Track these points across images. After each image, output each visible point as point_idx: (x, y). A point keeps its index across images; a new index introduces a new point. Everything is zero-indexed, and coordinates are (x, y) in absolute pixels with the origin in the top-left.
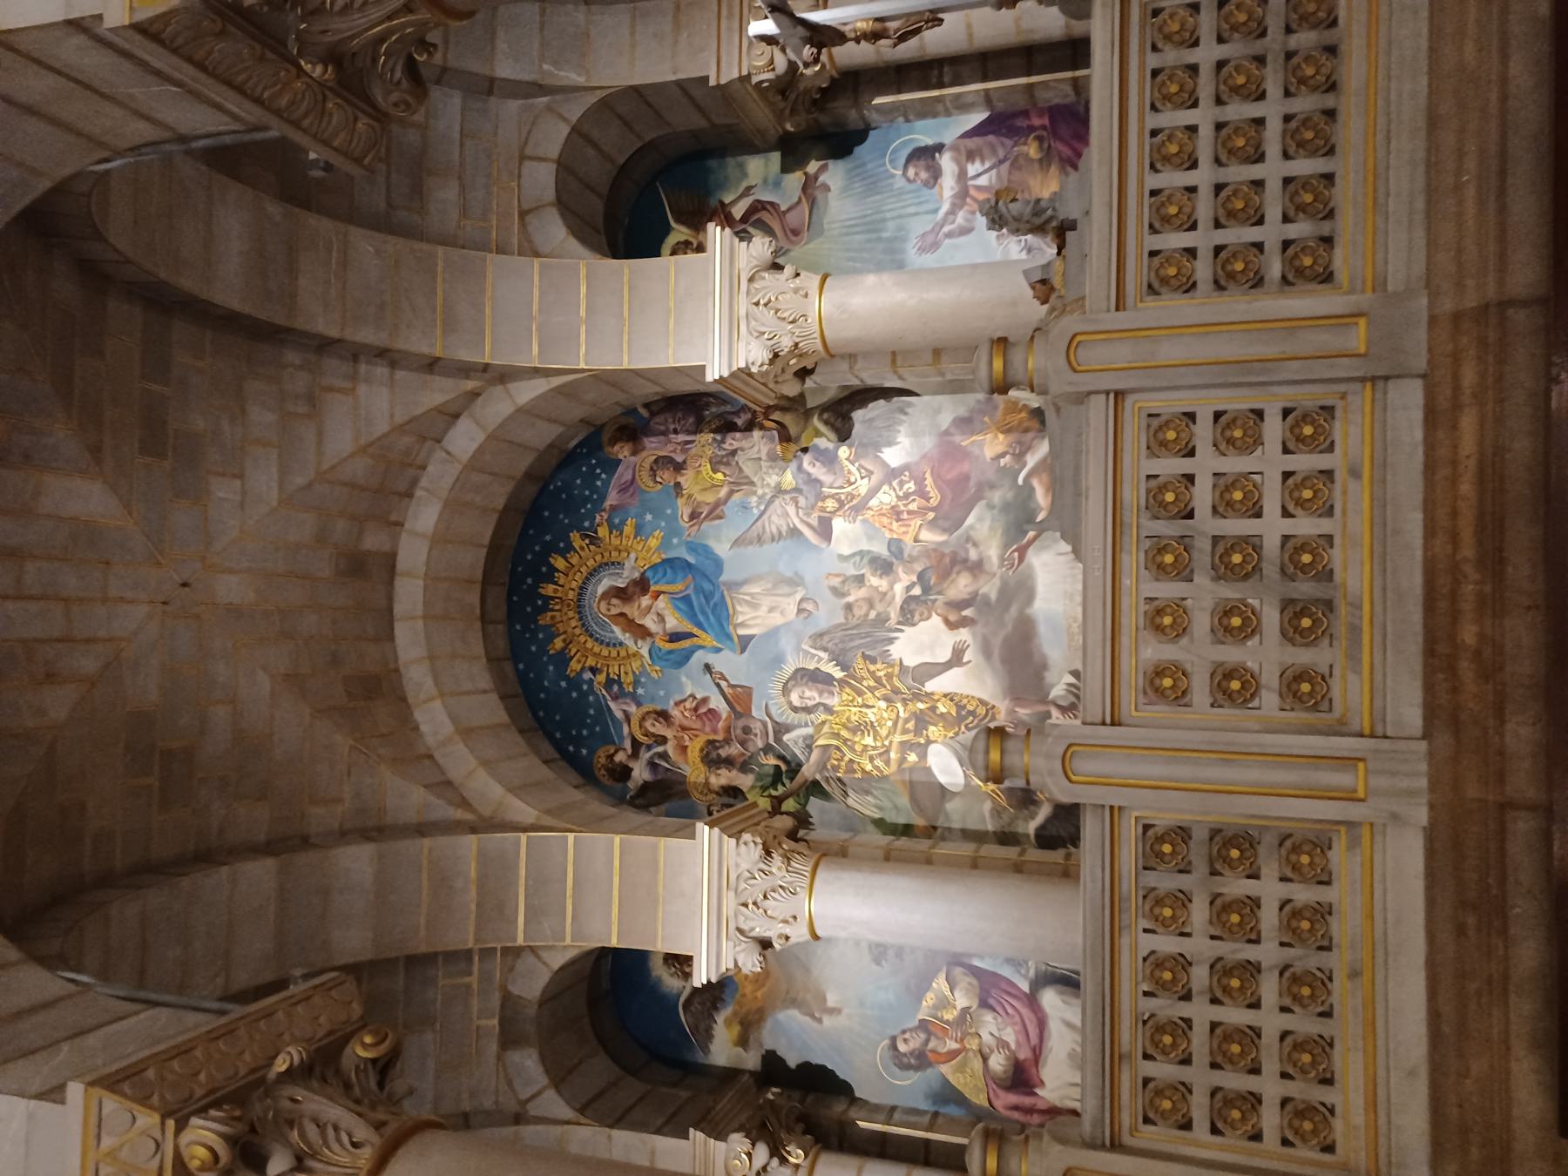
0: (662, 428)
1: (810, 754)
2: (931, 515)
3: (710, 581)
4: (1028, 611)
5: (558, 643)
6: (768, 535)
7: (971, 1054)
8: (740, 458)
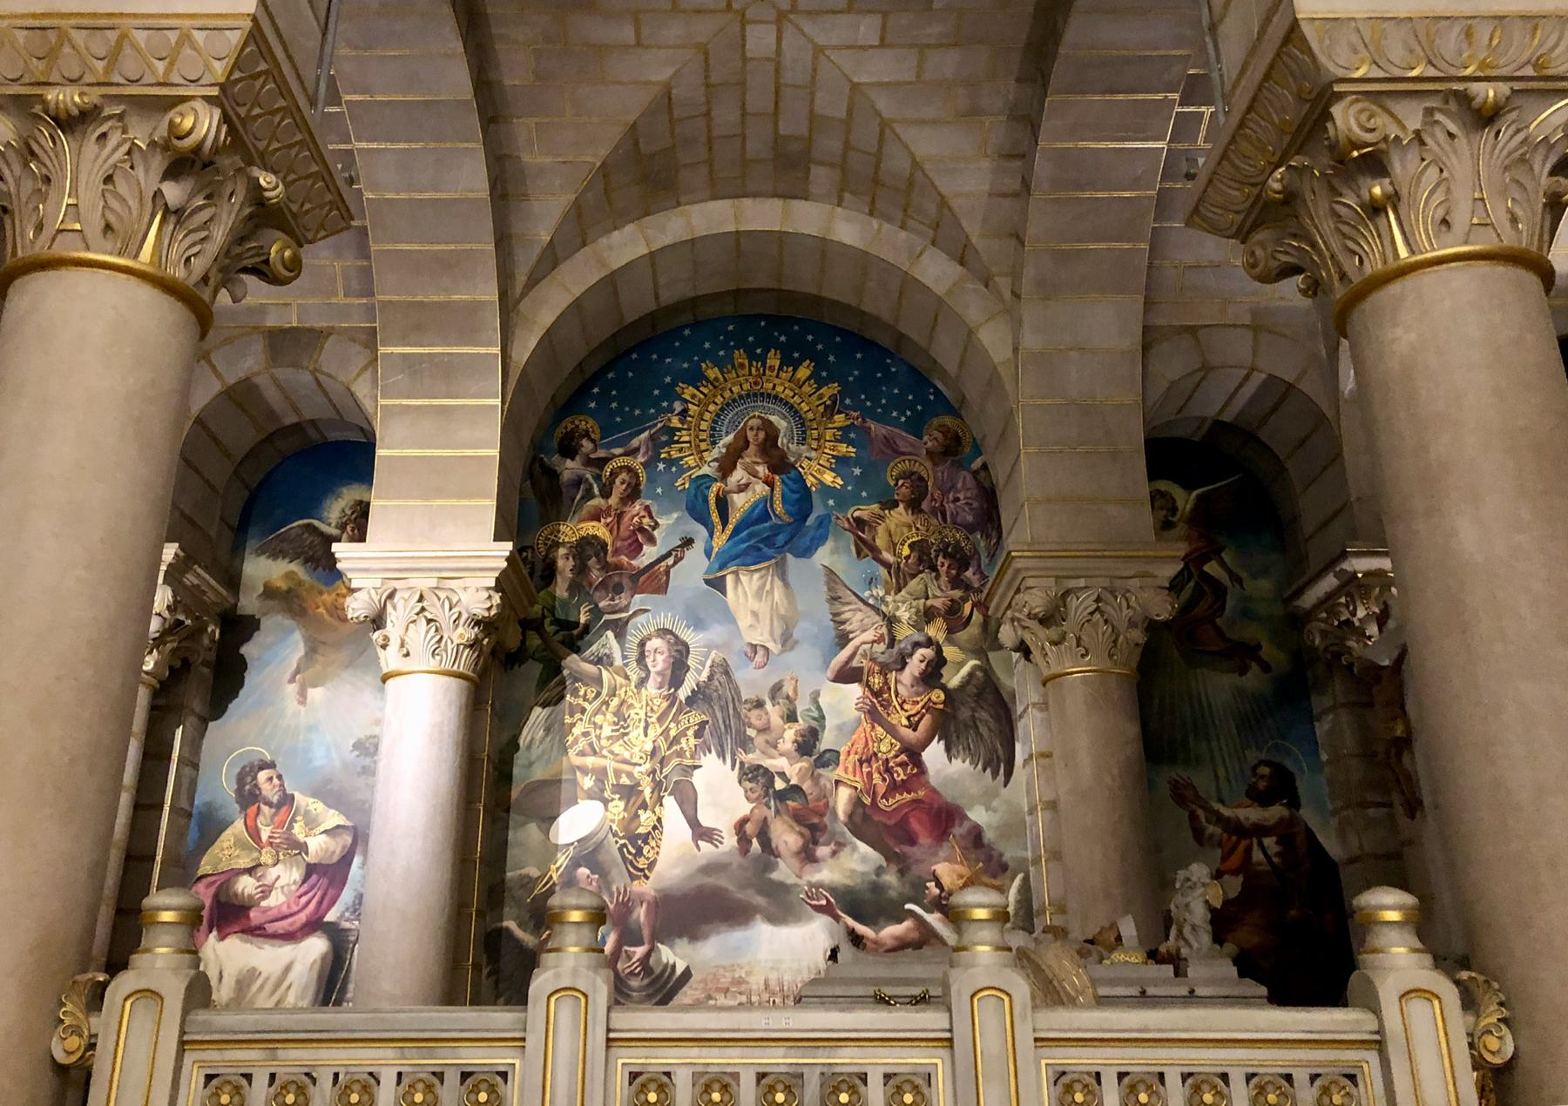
0: (960, 485)
1: (590, 662)
2: (867, 801)
4: (758, 917)
5: (713, 373)
6: (839, 608)
7: (256, 855)
8: (926, 576)
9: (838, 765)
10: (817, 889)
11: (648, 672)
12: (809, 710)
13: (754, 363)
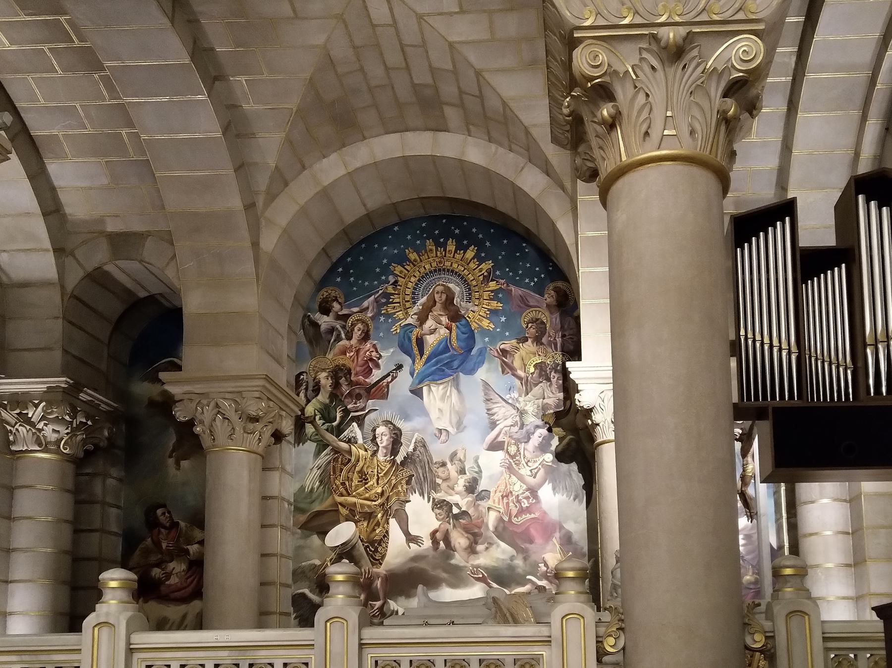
0: (566, 326)
1: (345, 442)
2: (506, 519)
3: (459, 366)
4: (444, 584)
5: (413, 256)
8: (544, 384)
9: (489, 499)
10: (477, 568)
11: (379, 447)
12: (473, 467)
13: (439, 248)
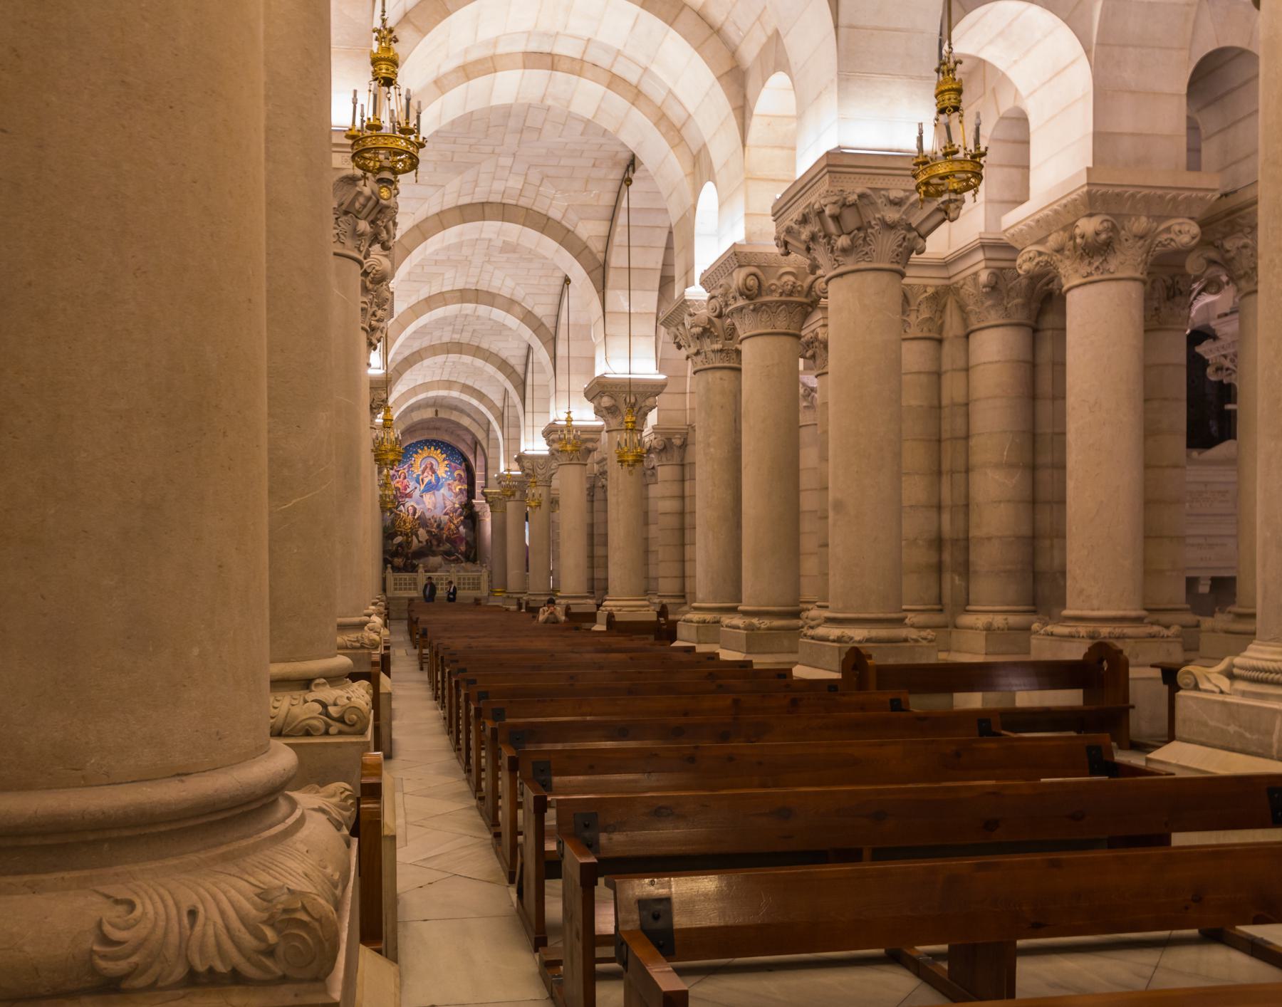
5: (420, 452)
